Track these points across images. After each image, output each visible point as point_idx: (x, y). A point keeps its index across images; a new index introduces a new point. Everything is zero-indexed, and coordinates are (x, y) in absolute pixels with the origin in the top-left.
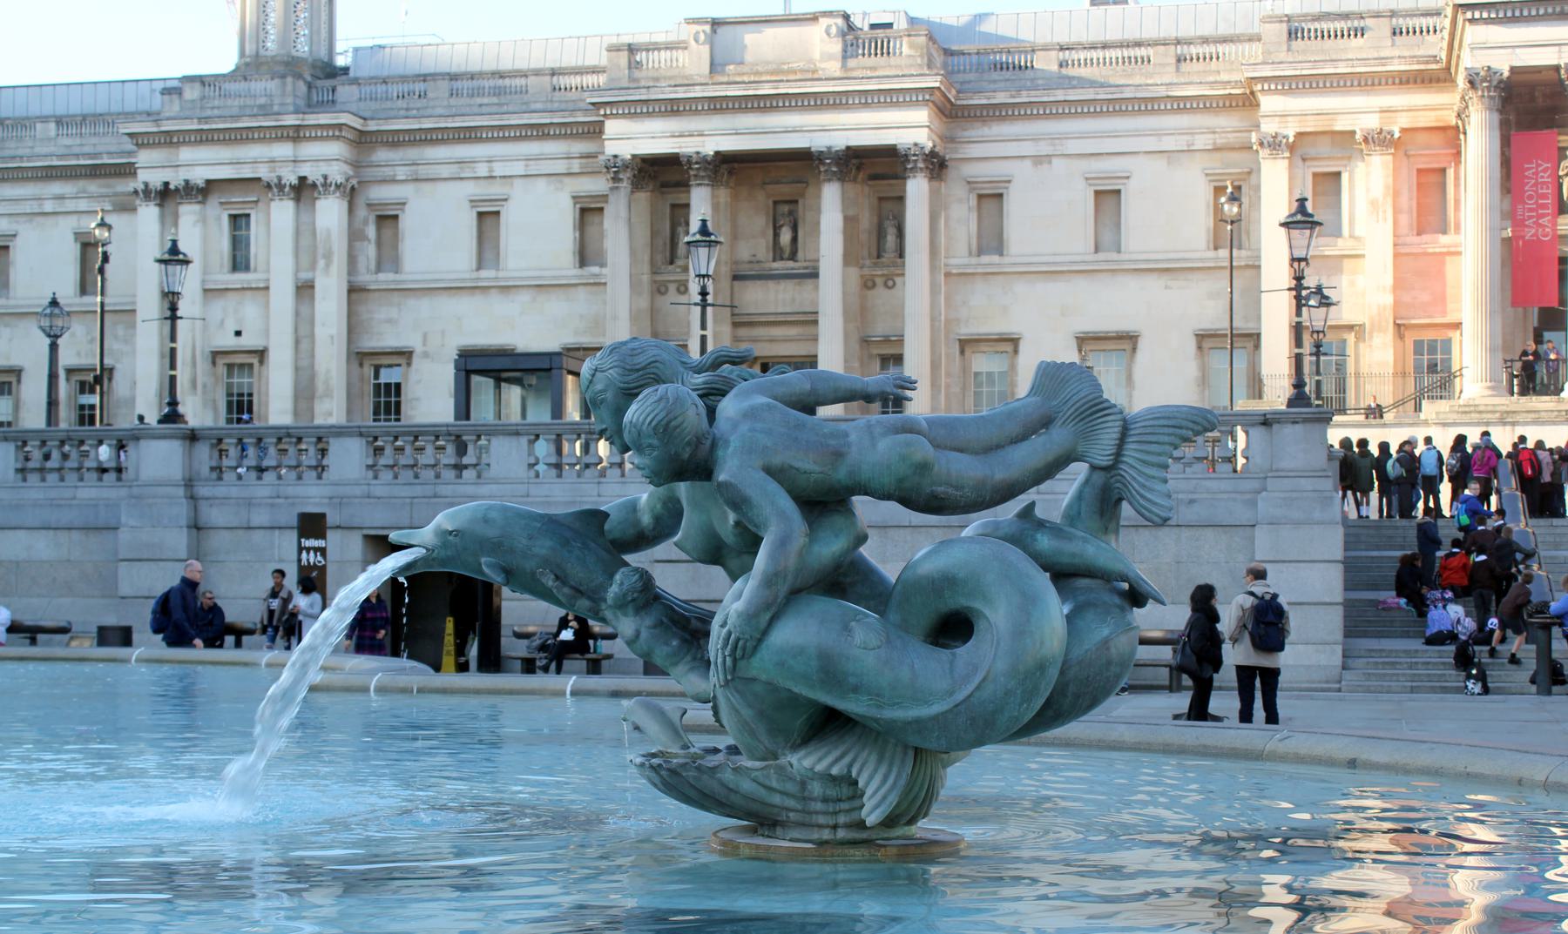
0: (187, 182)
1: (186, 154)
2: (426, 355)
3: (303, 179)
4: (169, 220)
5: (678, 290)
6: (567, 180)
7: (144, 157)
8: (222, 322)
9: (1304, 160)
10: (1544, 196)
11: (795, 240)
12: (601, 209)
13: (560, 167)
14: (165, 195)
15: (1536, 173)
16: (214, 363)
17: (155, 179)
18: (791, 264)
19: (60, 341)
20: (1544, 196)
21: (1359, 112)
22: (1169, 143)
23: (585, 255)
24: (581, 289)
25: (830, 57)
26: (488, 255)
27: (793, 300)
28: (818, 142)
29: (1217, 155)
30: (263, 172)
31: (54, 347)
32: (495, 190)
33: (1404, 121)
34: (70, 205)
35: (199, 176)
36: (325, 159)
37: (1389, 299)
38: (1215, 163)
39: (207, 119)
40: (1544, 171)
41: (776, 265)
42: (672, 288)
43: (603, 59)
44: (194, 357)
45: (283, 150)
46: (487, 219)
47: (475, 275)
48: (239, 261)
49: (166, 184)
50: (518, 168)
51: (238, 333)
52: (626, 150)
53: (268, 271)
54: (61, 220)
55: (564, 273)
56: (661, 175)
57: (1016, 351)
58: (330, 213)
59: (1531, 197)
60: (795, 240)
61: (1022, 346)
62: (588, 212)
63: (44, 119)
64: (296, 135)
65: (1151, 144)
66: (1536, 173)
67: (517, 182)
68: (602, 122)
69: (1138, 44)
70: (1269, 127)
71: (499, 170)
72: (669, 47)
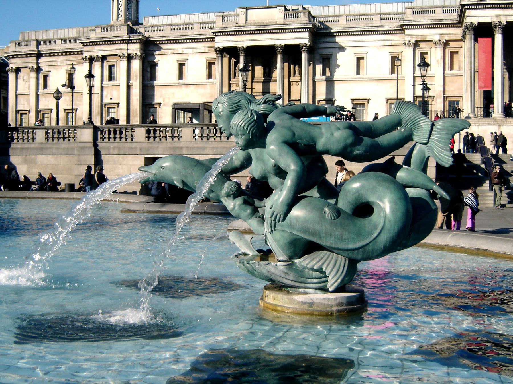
0: (97, 56)
1: (97, 48)
2: (164, 105)
3: (129, 55)
7: (86, 49)
13: (202, 50)
14: (91, 60)
17: (88, 55)
21: (434, 34)
23: (210, 76)
28: (277, 43)
30: (118, 52)
31: (58, 103)
32: (184, 57)
34: (65, 63)
35: (100, 54)
36: (135, 49)
39: (103, 38)
45: (124, 46)
48: (111, 78)
49: (91, 56)
50: (190, 51)
51: (111, 99)
52: (221, 45)
53: (119, 80)
54: (62, 67)
56: (232, 52)
58: (136, 64)
63: (58, 39)
64: (128, 42)
67: (190, 55)
68: (214, 38)
69: (370, 15)
70: (407, 39)
71: (185, 51)
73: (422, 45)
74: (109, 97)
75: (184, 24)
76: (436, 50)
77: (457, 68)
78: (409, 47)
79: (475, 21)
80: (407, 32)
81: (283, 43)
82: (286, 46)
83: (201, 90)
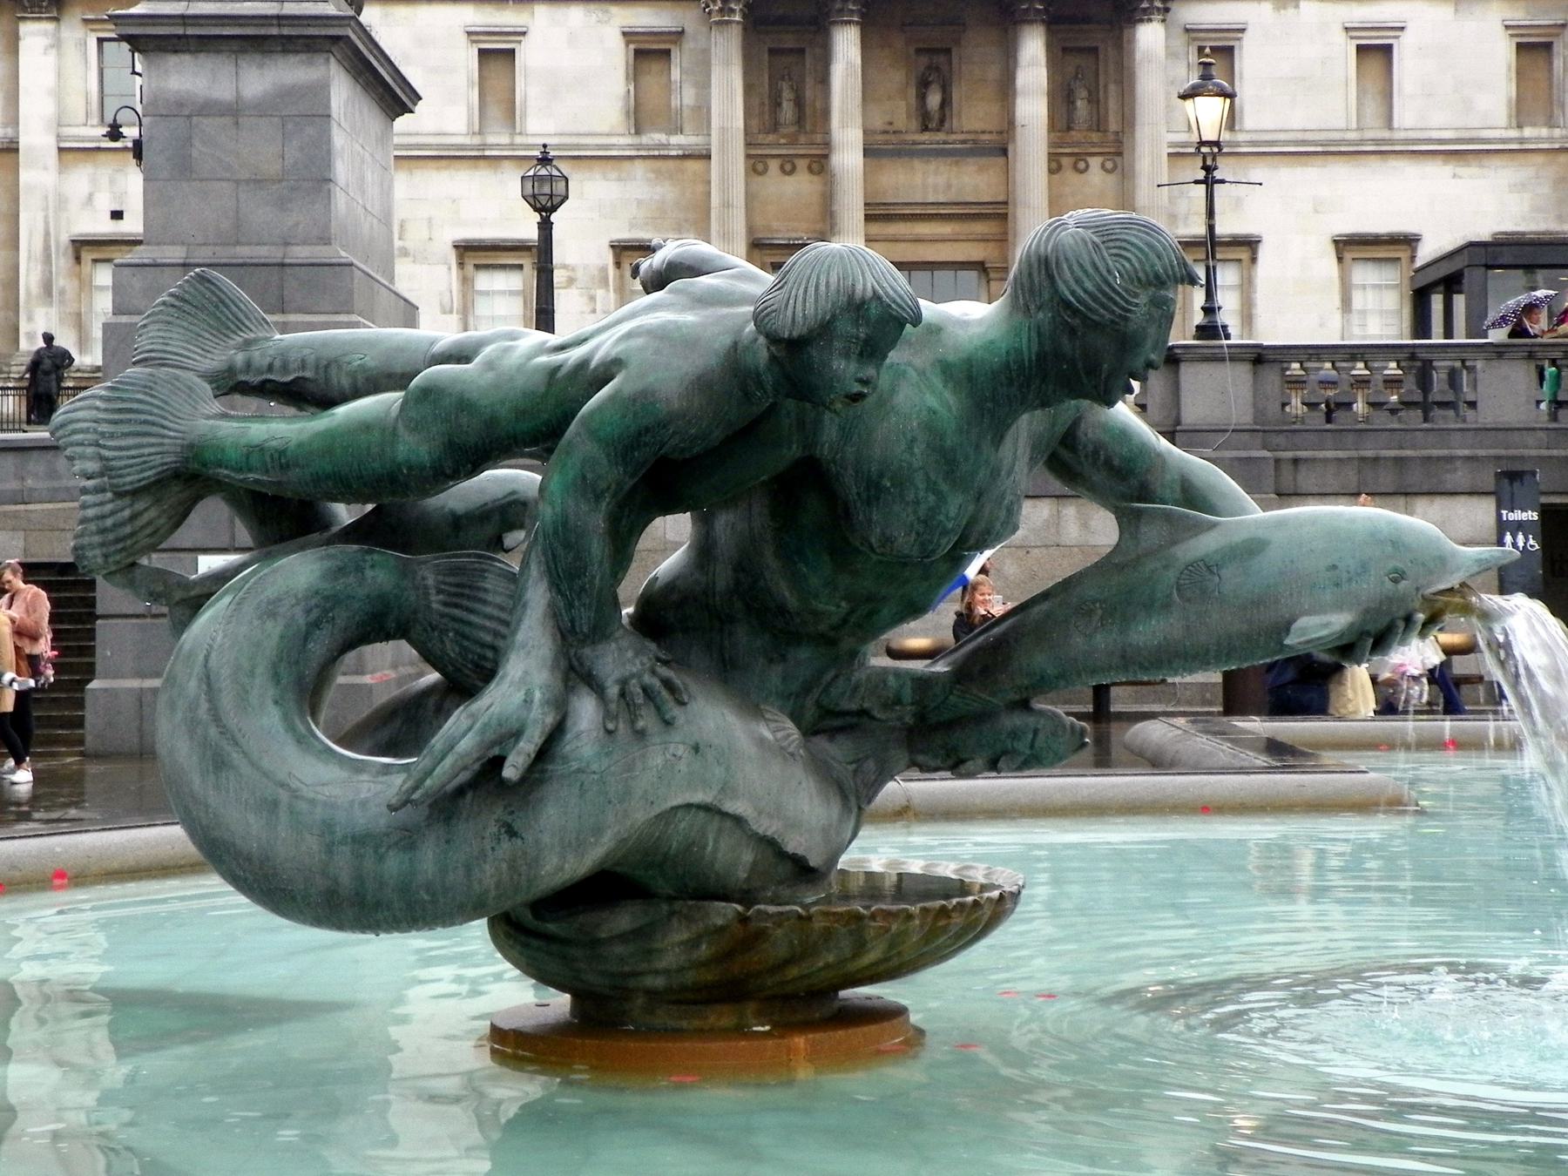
5: (782, 168)
8: (90, 198)
11: (945, 103)
12: (667, 53)
16: (78, 259)
18: (941, 136)
19: (554, 217)
24: (637, 163)
27: (949, 186)
42: (774, 165)
44: (47, 248)
51: (117, 215)
55: (614, 140)
57: (1254, 260)
60: (945, 103)
61: (1264, 252)
74: (105, 204)
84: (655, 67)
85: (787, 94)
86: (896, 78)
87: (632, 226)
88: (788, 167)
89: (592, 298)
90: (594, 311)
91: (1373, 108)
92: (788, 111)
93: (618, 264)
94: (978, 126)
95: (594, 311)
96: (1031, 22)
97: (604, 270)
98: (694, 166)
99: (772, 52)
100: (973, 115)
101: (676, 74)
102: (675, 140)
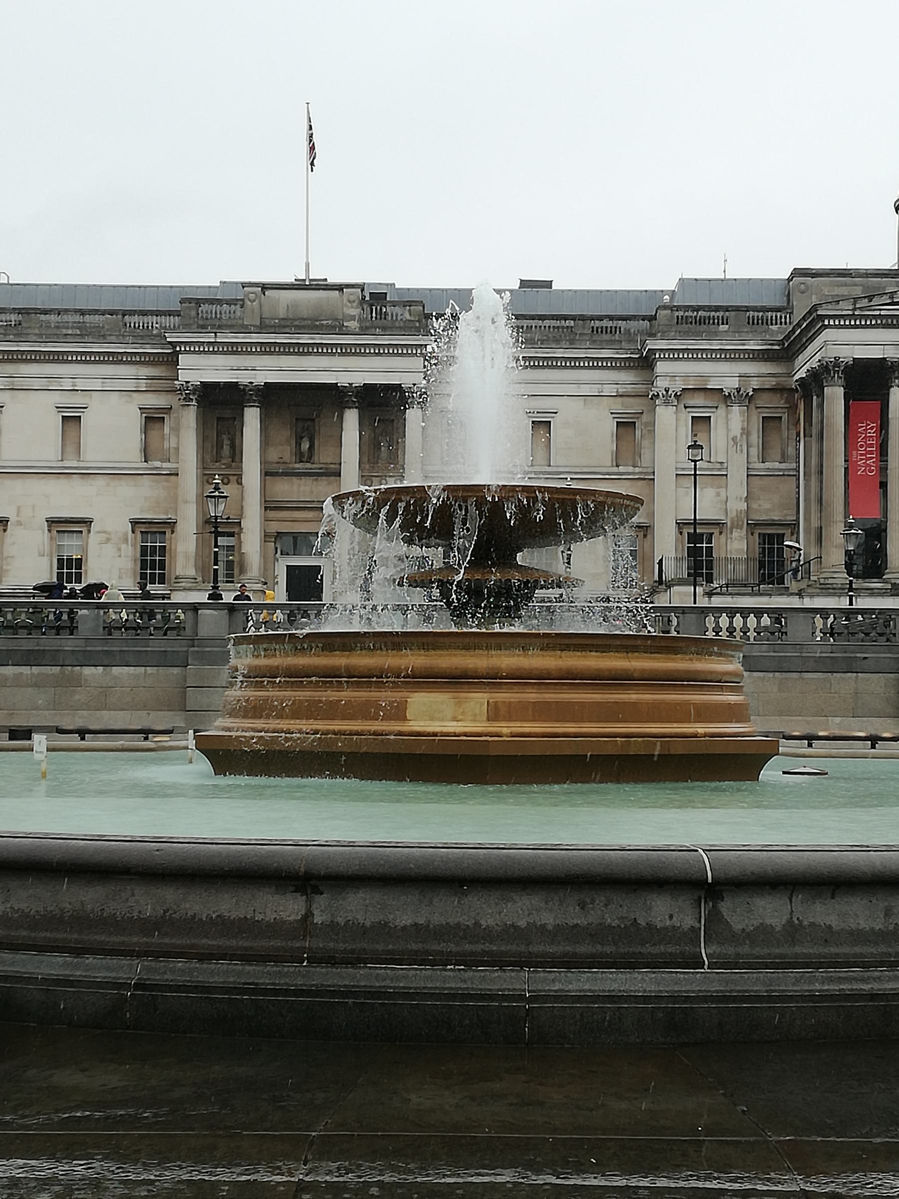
2: (19, 523)
4: (70, 449)
6: (134, 395)
9: (686, 407)
10: (871, 446)
11: (311, 447)
13: (130, 385)
15: (866, 430)
18: (308, 465)
20: (871, 446)
21: (726, 375)
22: (585, 390)
25: (353, 318)
26: (70, 449)
27: (312, 492)
28: (343, 380)
29: (619, 399)
33: (755, 383)
37: (744, 506)
38: (618, 406)
40: (872, 428)
41: (297, 466)
43: (177, 307)
46: (71, 421)
47: (60, 464)
50: (97, 385)
59: (862, 446)
60: (311, 447)
62: (153, 419)
65: (572, 390)
66: (866, 430)
69: (565, 318)
72: (230, 302)
73: (699, 400)
75: (76, 311)
76: (728, 413)
77: (779, 458)
78: (667, 403)
79: (848, 354)
80: (661, 367)
81: (359, 380)
82: (368, 388)
83: (126, 490)
84: (157, 425)
85: (226, 442)
86: (283, 434)
87: (142, 511)
88: (226, 481)
89: (119, 549)
90: (120, 556)
91: (541, 453)
92: (226, 450)
93: (133, 532)
94: (329, 460)
95: (120, 556)
96: (350, 408)
97: (126, 534)
98: (173, 477)
99: (218, 419)
100: (324, 456)
101: (167, 430)
102: (165, 465)
